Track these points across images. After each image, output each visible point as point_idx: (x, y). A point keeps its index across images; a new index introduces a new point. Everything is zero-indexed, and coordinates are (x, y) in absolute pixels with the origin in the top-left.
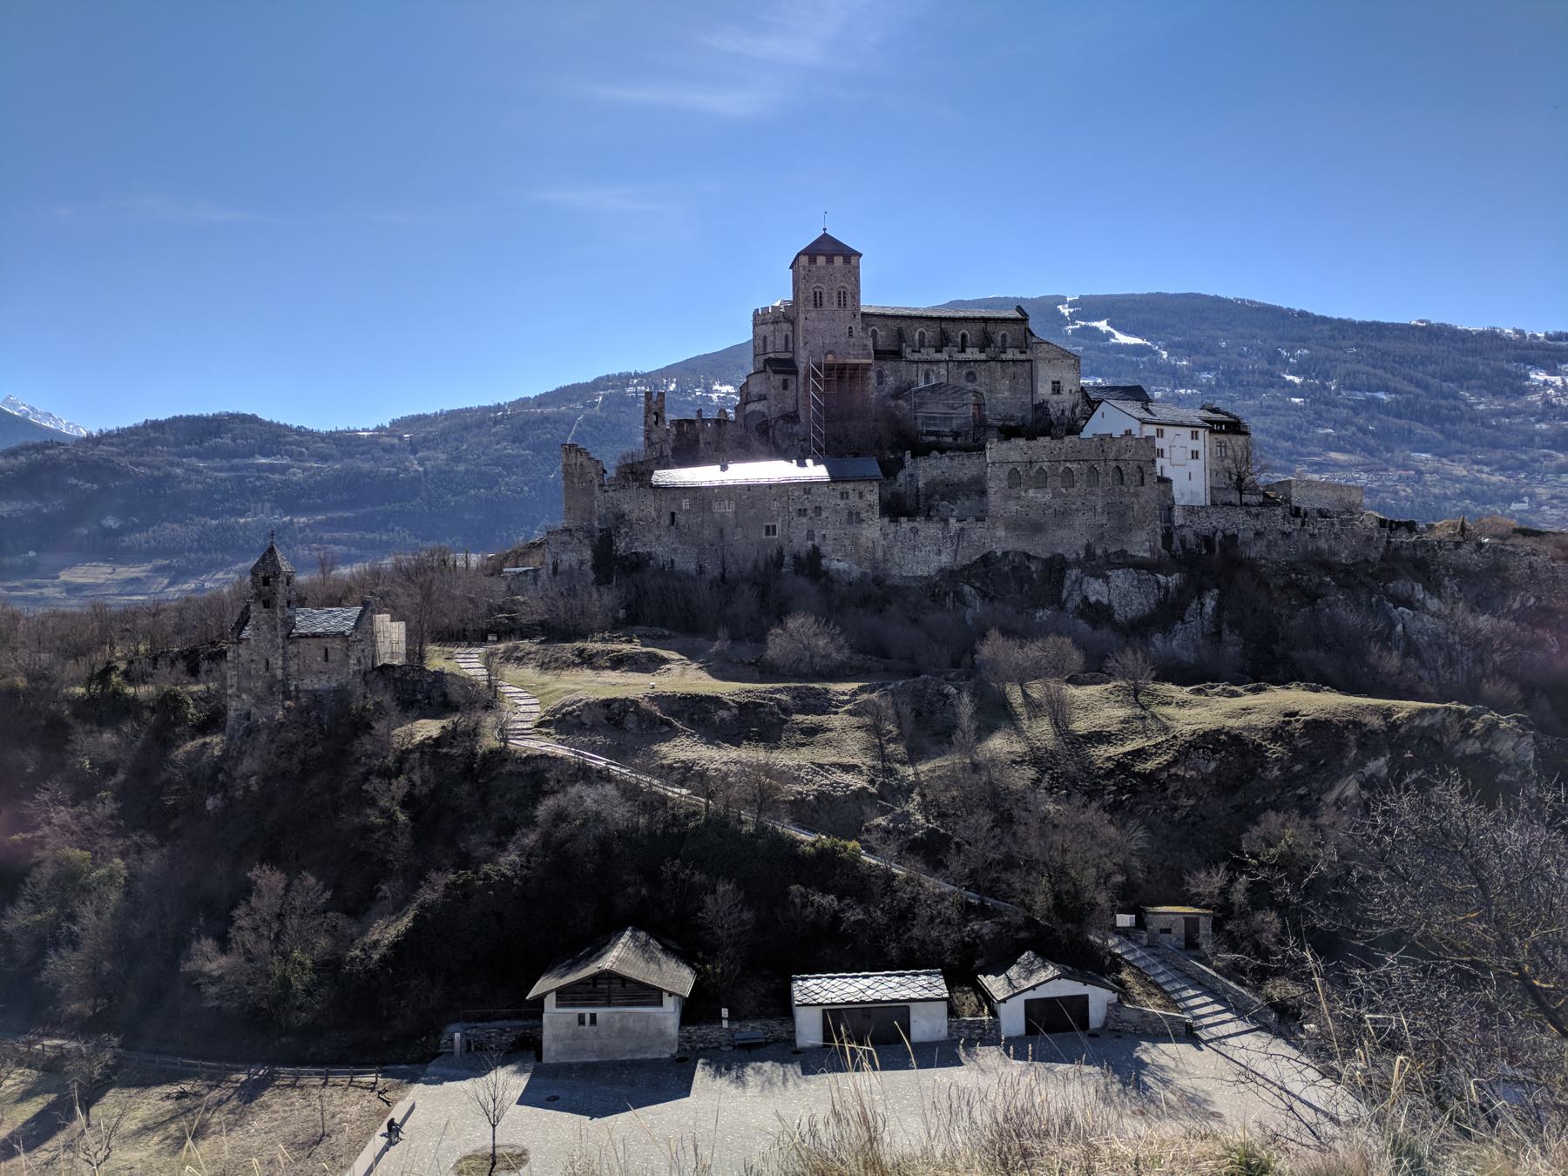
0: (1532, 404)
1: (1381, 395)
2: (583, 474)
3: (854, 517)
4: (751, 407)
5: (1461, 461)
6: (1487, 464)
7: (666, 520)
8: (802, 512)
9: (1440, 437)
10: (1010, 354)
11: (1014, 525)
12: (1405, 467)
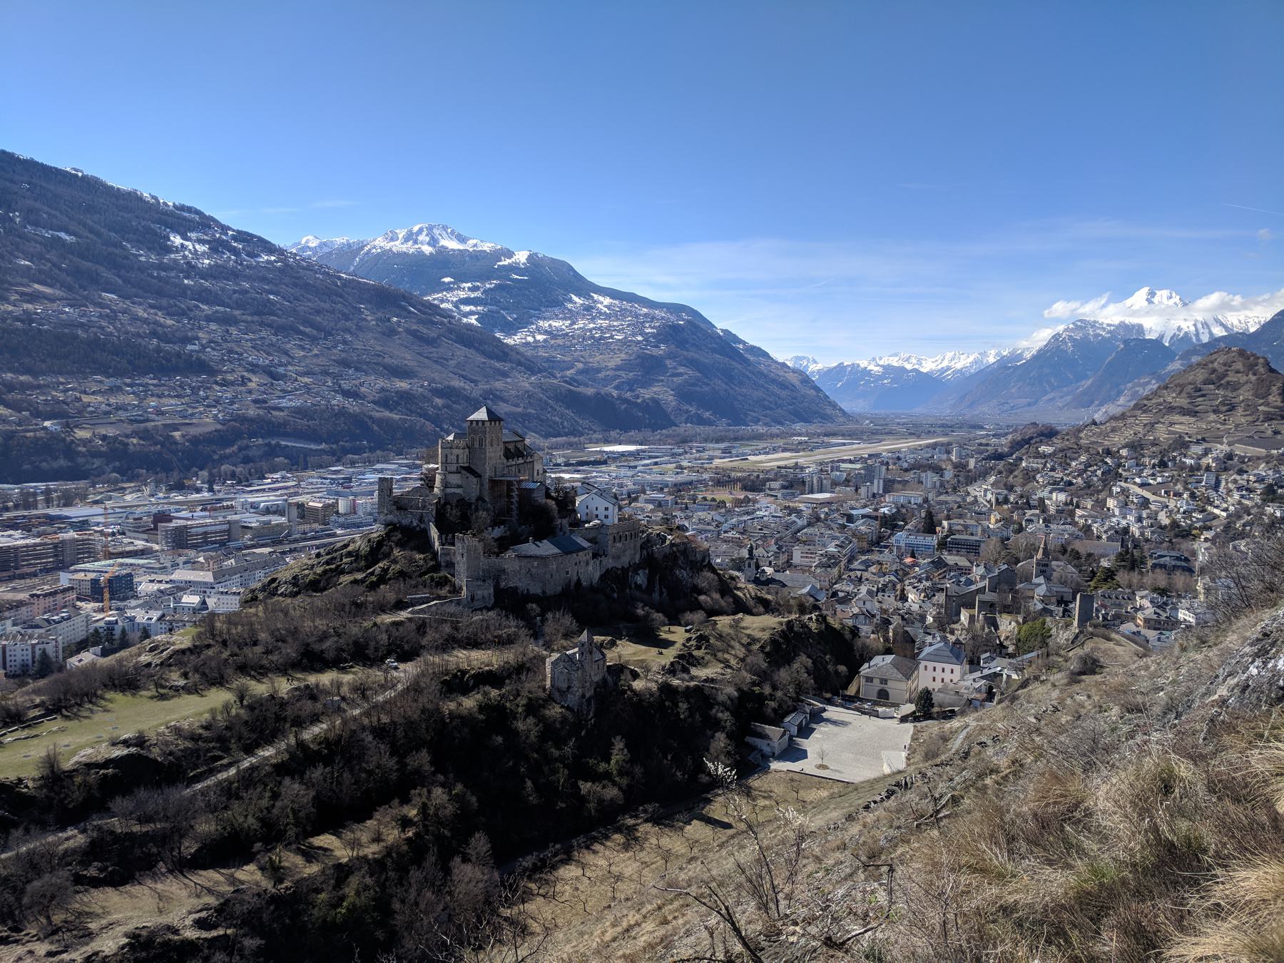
0: (175, 261)
1: (63, 235)
2: (476, 550)
3: (587, 564)
4: (448, 490)
5: (140, 304)
6: (160, 308)
9: (120, 282)
10: (529, 459)
11: (613, 558)
12: (101, 305)
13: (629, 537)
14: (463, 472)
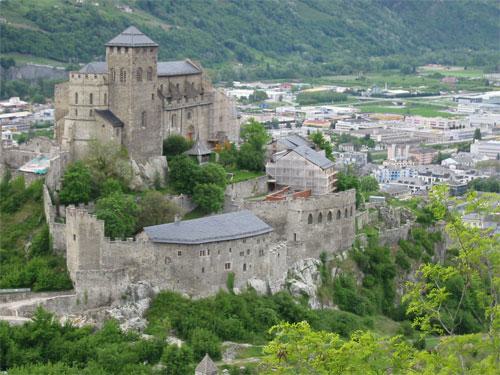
7: (161, 262)
8: (242, 254)
13: (334, 216)
14: (98, 117)
